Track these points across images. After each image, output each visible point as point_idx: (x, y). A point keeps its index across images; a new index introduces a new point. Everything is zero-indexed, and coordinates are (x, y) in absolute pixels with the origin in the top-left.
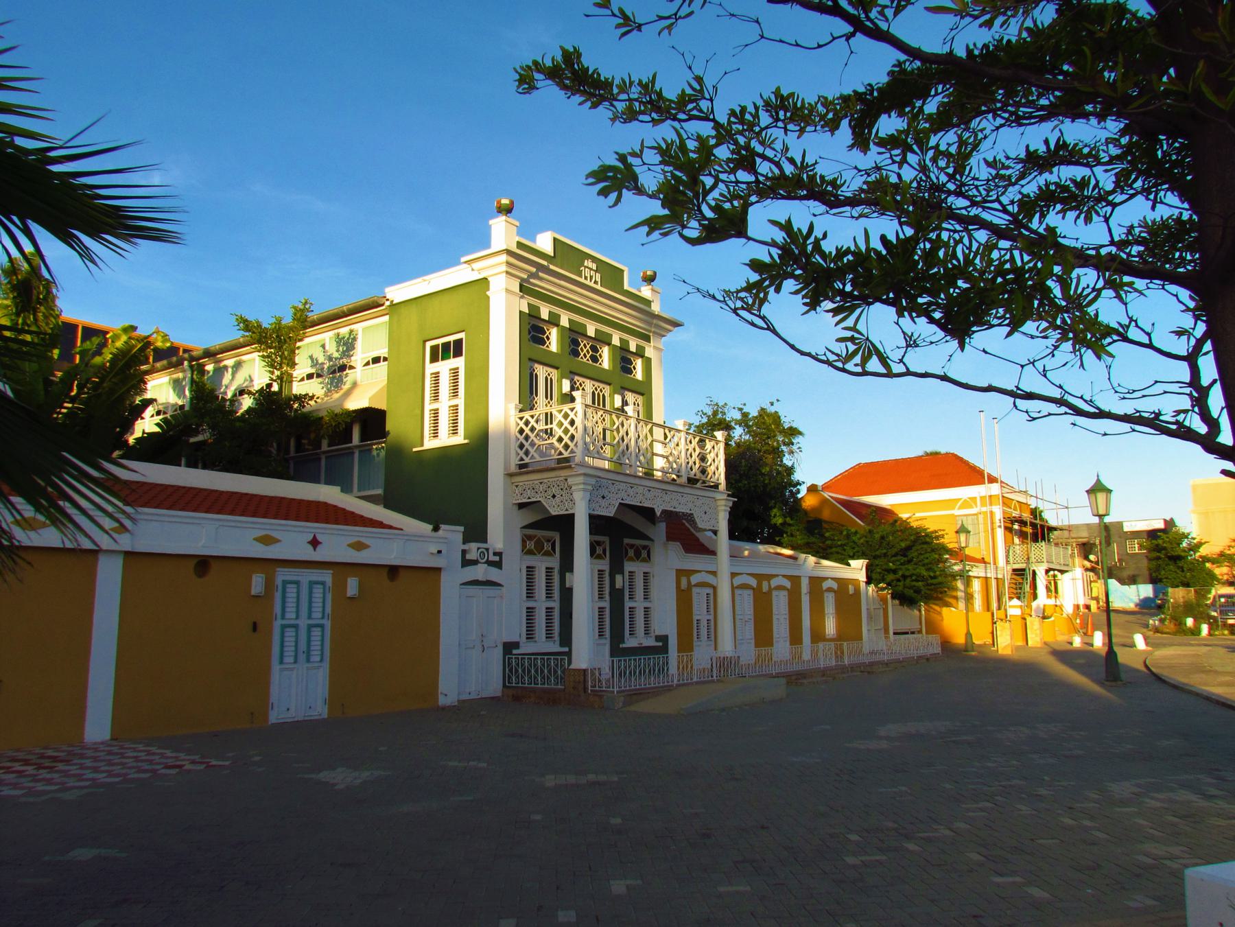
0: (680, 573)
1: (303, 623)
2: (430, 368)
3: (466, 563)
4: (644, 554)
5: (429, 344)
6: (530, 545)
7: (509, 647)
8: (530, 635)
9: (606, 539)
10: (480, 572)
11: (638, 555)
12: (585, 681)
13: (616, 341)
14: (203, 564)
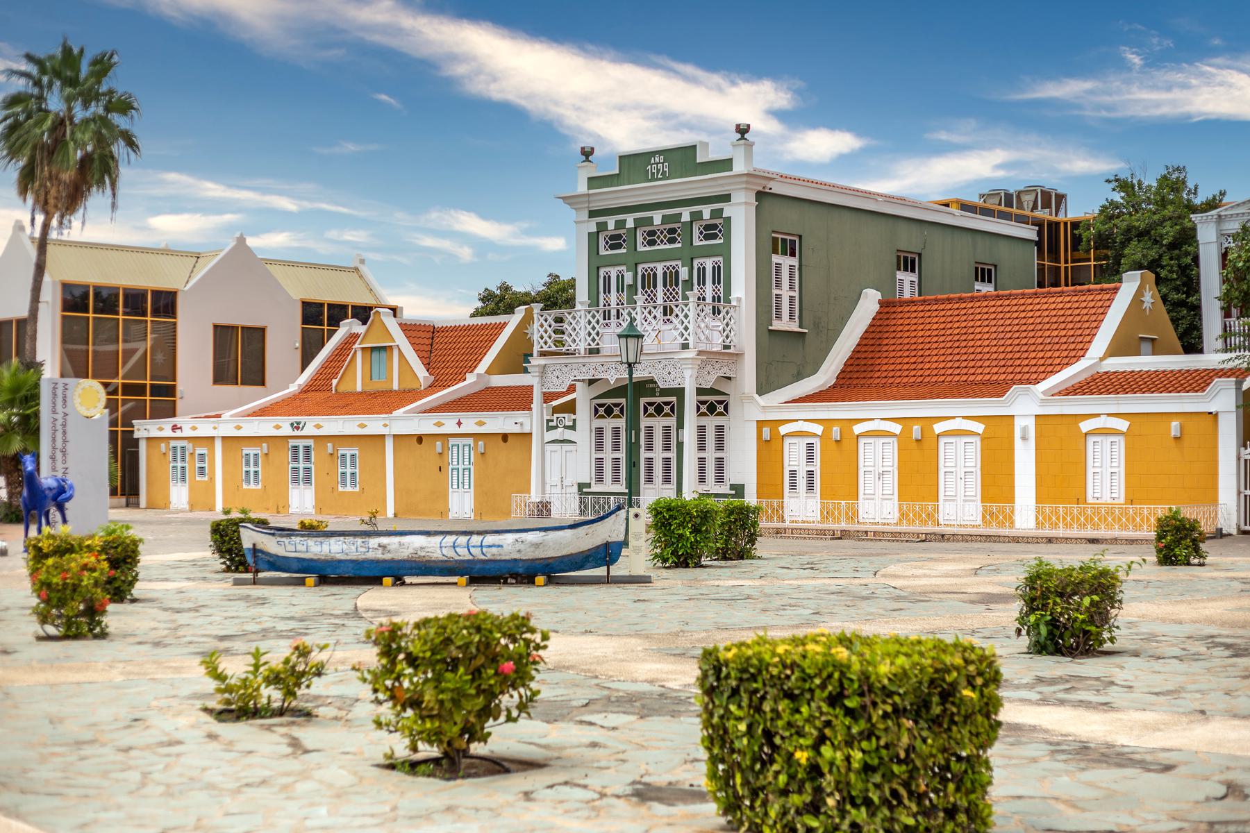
0: (761, 424)
1: (461, 467)
3: (549, 428)
4: (720, 408)
6: (601, 411)
7: (581, 486)
8: (600, 479)
14: (420, 439)
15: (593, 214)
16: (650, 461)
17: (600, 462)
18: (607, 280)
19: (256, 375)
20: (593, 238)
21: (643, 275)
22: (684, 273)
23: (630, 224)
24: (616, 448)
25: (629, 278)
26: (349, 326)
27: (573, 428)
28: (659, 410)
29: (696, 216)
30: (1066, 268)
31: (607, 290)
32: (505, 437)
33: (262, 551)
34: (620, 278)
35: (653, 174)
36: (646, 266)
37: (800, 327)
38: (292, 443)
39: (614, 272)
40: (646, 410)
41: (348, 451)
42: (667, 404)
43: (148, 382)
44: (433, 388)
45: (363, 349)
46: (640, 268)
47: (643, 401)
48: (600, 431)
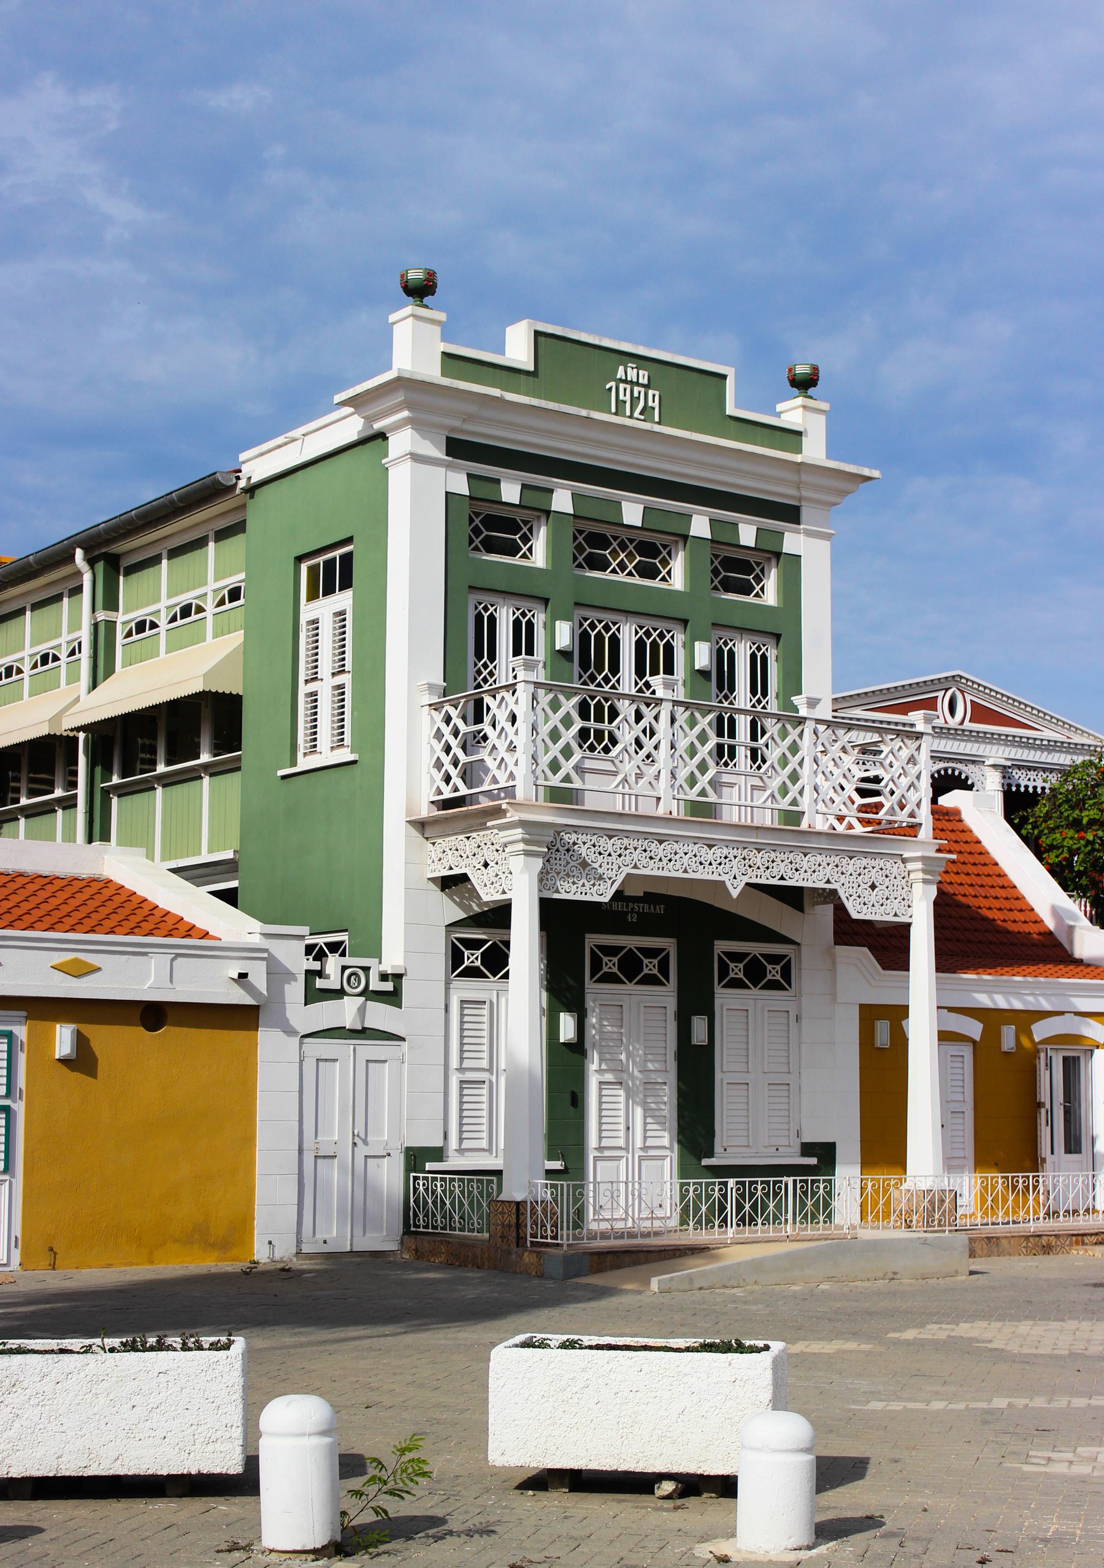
0: (870, 1014)
2: (308, 611)
3: (313, 995)
4: (773, 972)
5: (304, 568)
6: (472, 958)
9: (669, 944)
10: (346, 1012)
11: (755, 974)
12: (519, 1225)
13: (700, 526)
27: (393, 997)
28: (631, 968)
32: (153, 1015)
35: (620, 403)
36: (593, 615)
40: (596, 965)
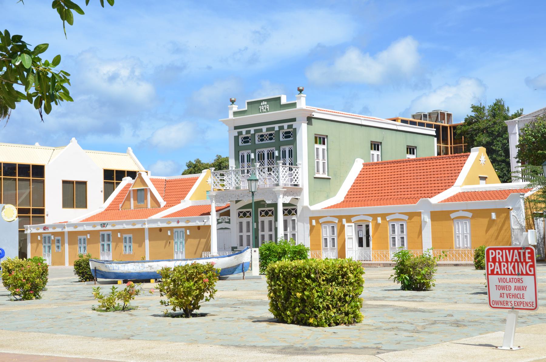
4: (293, 212)
6: (241, 215)
14: (161, 229)
15: (236, 128)
16: (263, 236)
17: (241, 237)
18: (243, 157)
19: (83, 203)
20: (236, 138)
21: (259, 155)
22: (276, 154)
23: (252, 132)
24: (248, 231)
25: (252, 156)
26: (127, 180)
27: (229, 222)
28: (267, 213)
29: (281, 128)
30: (451, 147)
31: (243, 161)
33: (99, 271)
34: (249, 156)
35: (262, 110)
36: (260, 150)
37: (328, 175)
38: (101, 233)
39: (245, 153)
40: (261, 214)
41: (128, 236)
42: (270, 211)
43: (31, 208)
44: (166, 207)
45: (133, 190)
46: (257, 151)
47: (260, 209)
48: (241, 223)
